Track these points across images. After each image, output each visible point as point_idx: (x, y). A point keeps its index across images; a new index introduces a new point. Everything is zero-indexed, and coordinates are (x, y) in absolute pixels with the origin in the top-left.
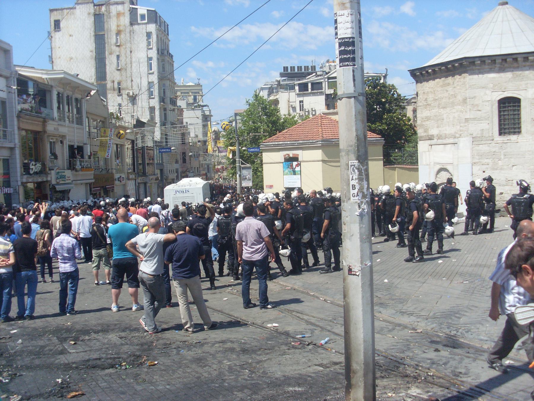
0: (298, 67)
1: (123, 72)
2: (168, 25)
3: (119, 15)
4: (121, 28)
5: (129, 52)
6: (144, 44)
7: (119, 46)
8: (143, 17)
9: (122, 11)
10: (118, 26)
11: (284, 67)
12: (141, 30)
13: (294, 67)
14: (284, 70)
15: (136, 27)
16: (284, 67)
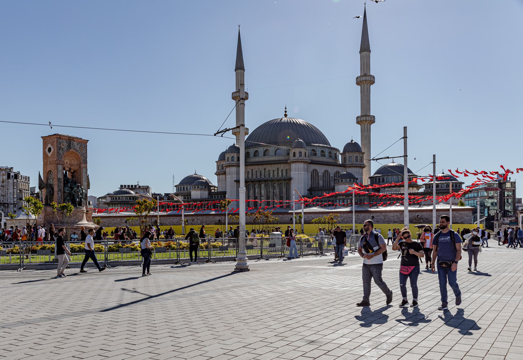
0: (128, 185)
1: (5, 198)
2: (29, 177)
3: (3, 175)
4: (4, 180)
5: (7, 190)
6: (12, 187)
7: (3, 187)
8: (12, 176)
9: (5, 174)
10: (3, 179)
11: (121, 185)
12: (11, 181)
13: (126, 185)
14: (121, 187)
15: (10, 180)
16: (121, 185)
